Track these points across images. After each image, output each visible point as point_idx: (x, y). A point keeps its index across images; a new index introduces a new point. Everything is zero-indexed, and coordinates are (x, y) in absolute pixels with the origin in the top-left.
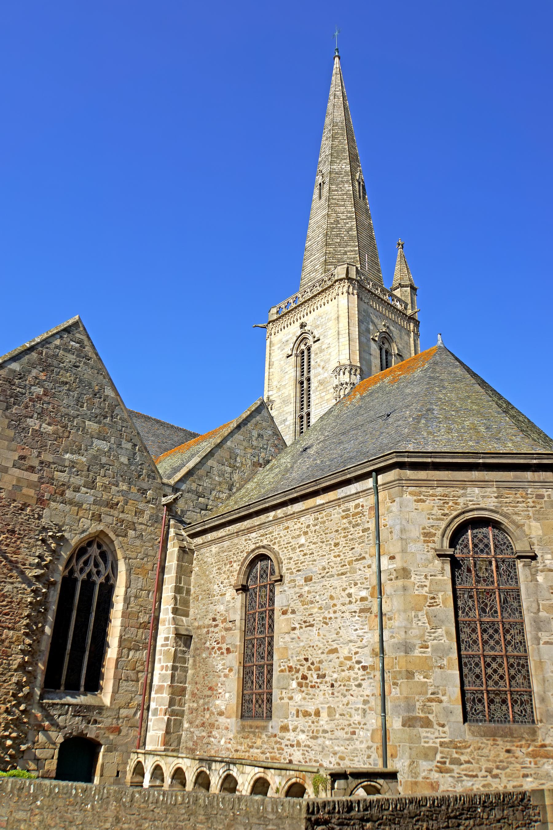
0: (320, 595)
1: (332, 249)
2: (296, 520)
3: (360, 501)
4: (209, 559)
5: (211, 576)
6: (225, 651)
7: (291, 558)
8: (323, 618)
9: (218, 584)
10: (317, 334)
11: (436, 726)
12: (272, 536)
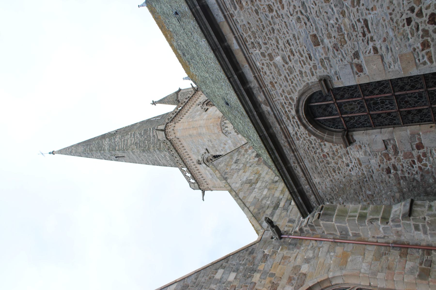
0: (329, 19)
1: (152, 146)
2: (261, 73)
4: (328, 185)
5: (344, 180)
6: (422, 151)
7: (301, 73)
8: (354, 7)
9: (350, 171)
10: (203, 151)
12: (285, 103)
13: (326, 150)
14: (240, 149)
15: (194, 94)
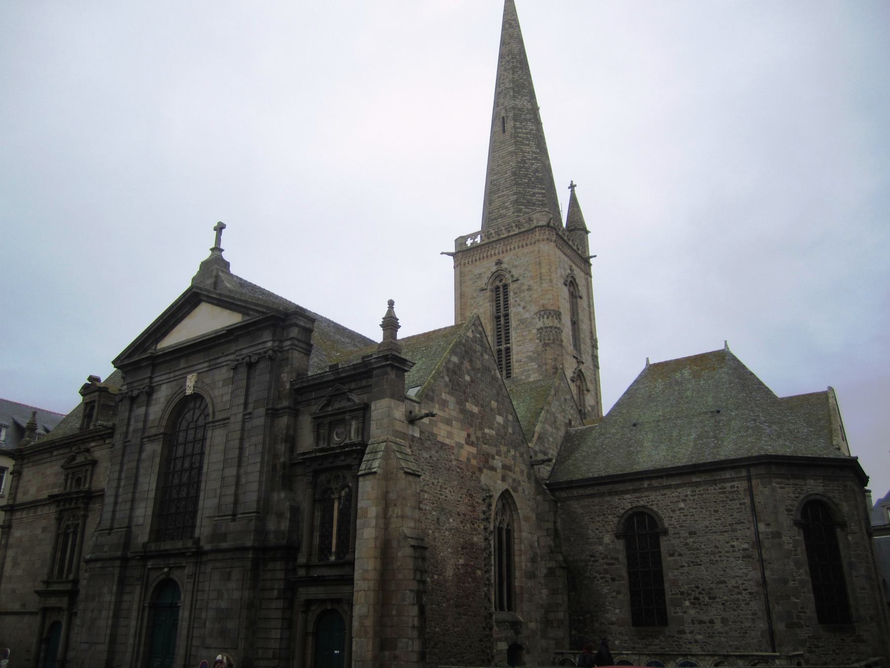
0: (705, 545)
3: (736, 484)
10: (515, 273)
11: (805, 627)
13: (610, 517)
14: (573, 400)
15: (582, 258)
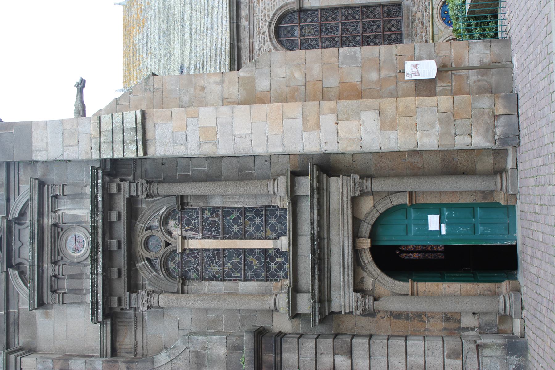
12: (262, 19)
